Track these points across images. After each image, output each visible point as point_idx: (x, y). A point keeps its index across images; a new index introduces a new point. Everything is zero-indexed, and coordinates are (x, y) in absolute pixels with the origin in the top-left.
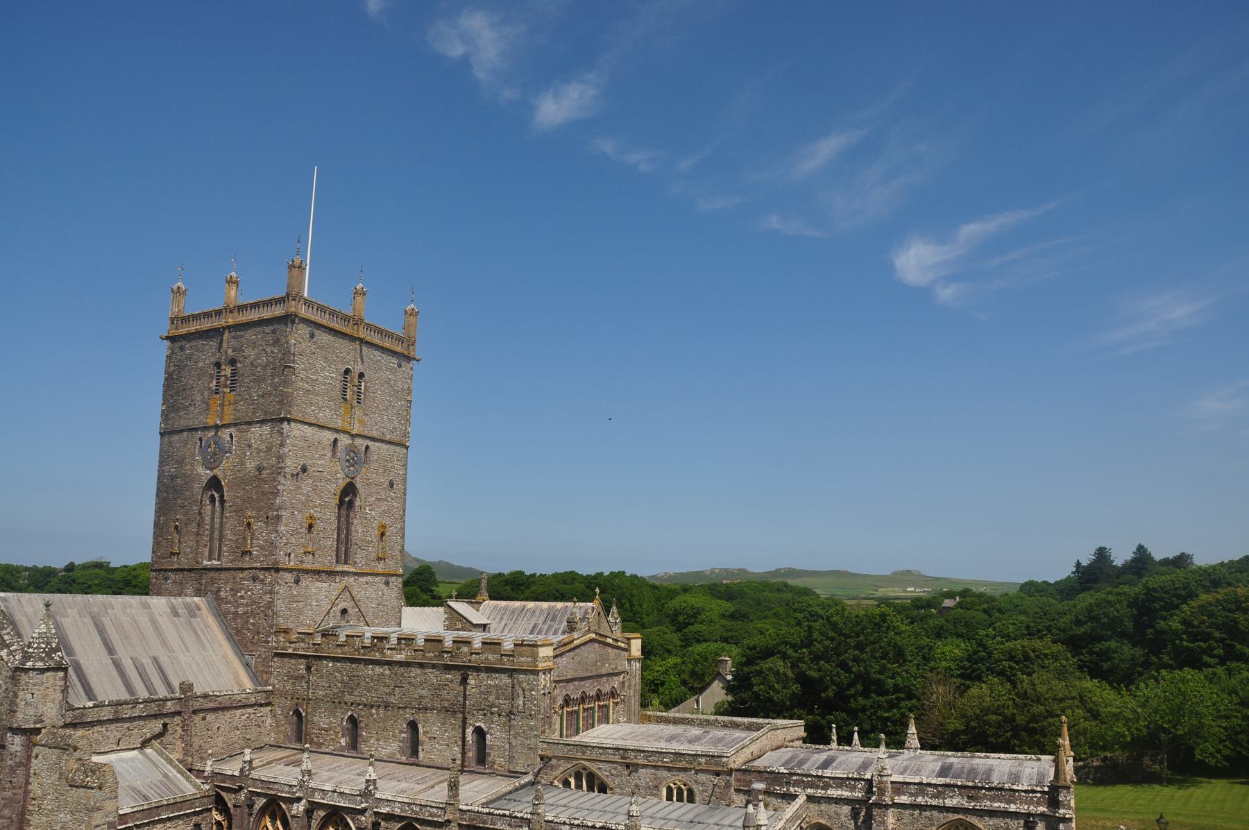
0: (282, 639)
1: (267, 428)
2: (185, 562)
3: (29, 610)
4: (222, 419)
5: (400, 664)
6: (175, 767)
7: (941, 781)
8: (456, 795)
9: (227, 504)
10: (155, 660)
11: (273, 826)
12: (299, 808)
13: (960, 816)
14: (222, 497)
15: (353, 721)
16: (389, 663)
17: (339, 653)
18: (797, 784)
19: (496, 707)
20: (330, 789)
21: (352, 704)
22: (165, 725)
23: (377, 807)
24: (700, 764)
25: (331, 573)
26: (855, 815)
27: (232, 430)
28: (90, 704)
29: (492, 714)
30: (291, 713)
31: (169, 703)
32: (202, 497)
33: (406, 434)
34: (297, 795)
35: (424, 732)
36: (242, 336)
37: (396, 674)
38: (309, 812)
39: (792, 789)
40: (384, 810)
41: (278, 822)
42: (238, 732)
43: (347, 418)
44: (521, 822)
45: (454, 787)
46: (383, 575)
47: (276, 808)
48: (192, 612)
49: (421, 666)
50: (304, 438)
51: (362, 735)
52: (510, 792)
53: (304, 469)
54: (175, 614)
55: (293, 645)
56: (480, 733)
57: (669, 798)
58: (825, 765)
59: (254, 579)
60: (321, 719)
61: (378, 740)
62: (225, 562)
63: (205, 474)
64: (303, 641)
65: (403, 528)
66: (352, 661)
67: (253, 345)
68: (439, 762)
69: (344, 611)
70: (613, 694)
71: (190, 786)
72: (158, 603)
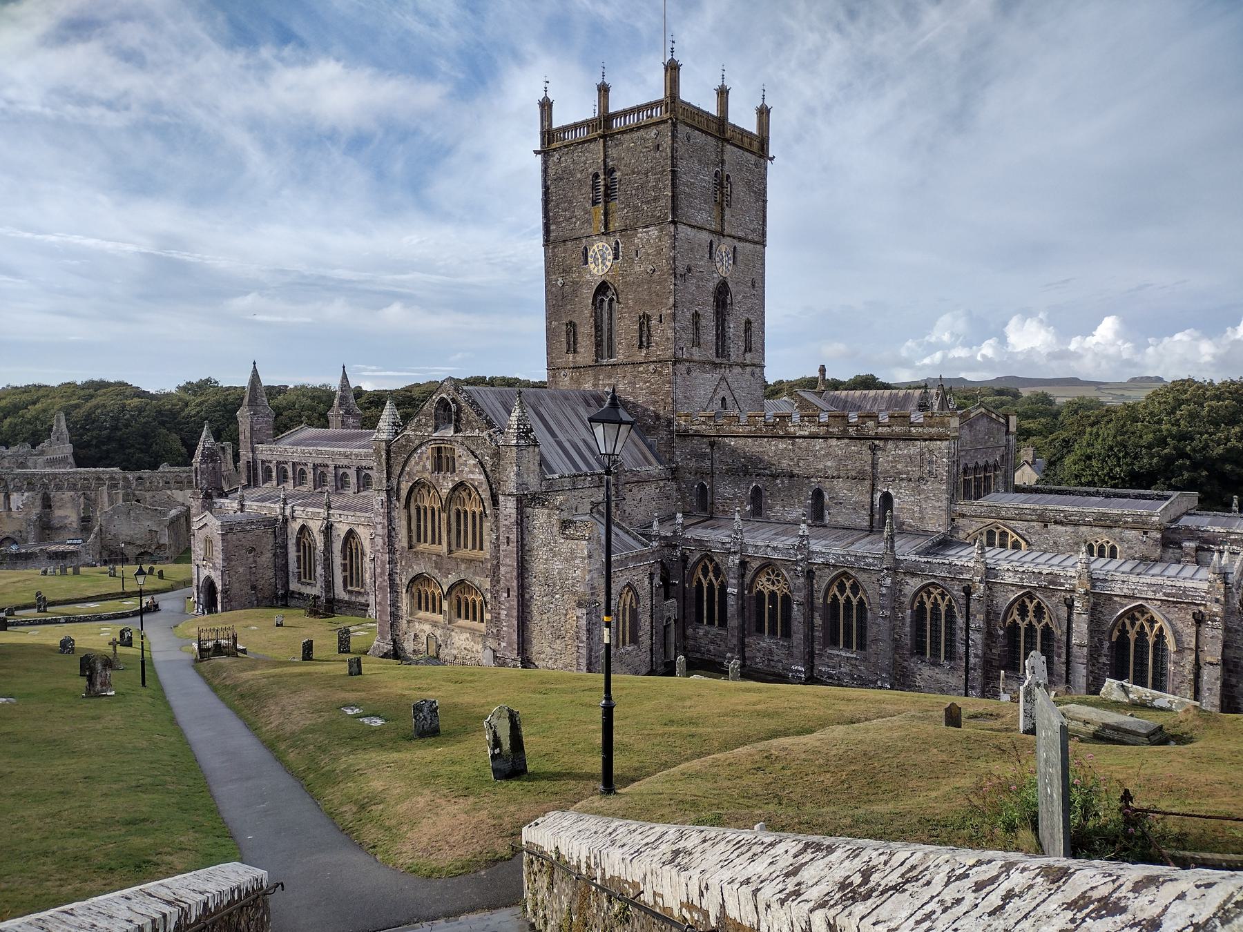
0: (683, 423)
1: (654, 232)
3: (488, 401)
4: (606, 226)
8: (892, 547)
10: (584, 441)
11: (705, 578)
15: (757, 494)
19: (905, 473)
20: (762, 544)
21: (757, 475)
23: (811, 559)
24: (1126, 522)
25: (716, 366)
28: (556, 476)
29: (902, 480)
30: (696, 486)
32: (593, 302)
33: (764, 234)
34: (733, 550)
35: (830, 498)
37: (800, 448)
38: (743, 564)
41: (711, 574)
42: (654, 503)
43: (718, 220)
44: (961, 569)
47: (708, 563)
50: (688, 241)
51: (766, 503)
52: (930, 547)
53: (689, 270)
55: (694, 428)
56: (887, 498)
60: (725, 490)
61: (784, 506)
62: (620, 357)
64: (704, 423)
65: (763, 324)
69: (724, 399)
70: (996, 467)
71: (639, 545)
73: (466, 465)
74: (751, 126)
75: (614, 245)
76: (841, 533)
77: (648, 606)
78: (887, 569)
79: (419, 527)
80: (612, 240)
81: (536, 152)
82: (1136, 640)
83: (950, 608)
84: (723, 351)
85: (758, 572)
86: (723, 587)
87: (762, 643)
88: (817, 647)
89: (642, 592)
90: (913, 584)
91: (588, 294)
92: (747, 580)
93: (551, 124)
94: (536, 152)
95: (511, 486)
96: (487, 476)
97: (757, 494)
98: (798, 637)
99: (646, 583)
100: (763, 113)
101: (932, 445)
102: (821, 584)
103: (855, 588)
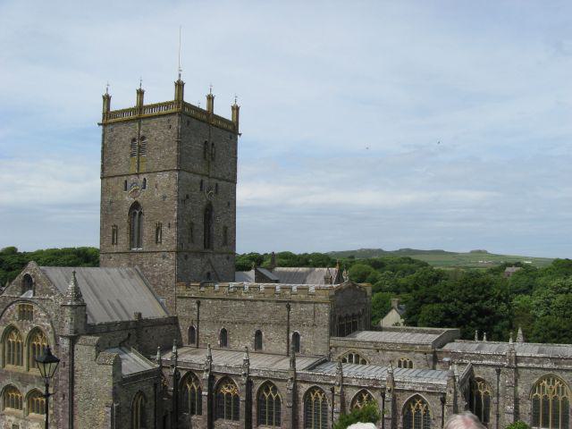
1: (167, 175)
2: (120, 248)
5: (251, 300)
6: (139, 356)
7: (542, 355)
9: (145, 217)
10: (118, 301)
12: (206, 375)
13: (551, 372)
14: (141, 213)
15: (224, 332)
16: (244, 300)
17: (215, 296)
18: (466, 358)
22: (129, 335)
25: (202, 254)
26: (499, 372)
27: (145, 176)
31: (131, 324)
36: (148, 124)
38: (212, 377)
39: (464, 361)
40: (254, 374)
41: (193, 384)
45: (293, 362)
46: (226, 253)
48: (131, 275)
49: (263, 301)
53: (187, 197)
54: (123, 277)
56: (296, 336)
57: (400, 366)
58: (479, 348)
59: (164, 257)
60: (205, 331)
63: (129, 200)
66: (224, 299)
67: (155, 128)
68: (274, 351)
69: (209, 274)
70: (359, 316)
72: (114, 271)
73: (40, 316)
74: (228, 115)
75: (142, 180)
76: (270, 357)
77: (153, 404)
78: (292, 379)
79: (9, 354)
80: (142, 177)
81: (99, 124)
82: (416, 414)
83: (324, 399)
84: (209, 245)
85: (221, 382)
86: (200, 390)
87: (223, 425)
88: (254, 426)
89: (149, 396)
90: (304, 388)
91: (126, 210)
92: (214, 386)
93: (108, 109)
94: (99, 124)
95: (67, 330)
96: (52, 324)
97: (224, 332)
98: (243, 420)
99: (152, 389)
100: (236, 109)
101: (320, 305)
102: (255, 389)
103: (275, 389)
